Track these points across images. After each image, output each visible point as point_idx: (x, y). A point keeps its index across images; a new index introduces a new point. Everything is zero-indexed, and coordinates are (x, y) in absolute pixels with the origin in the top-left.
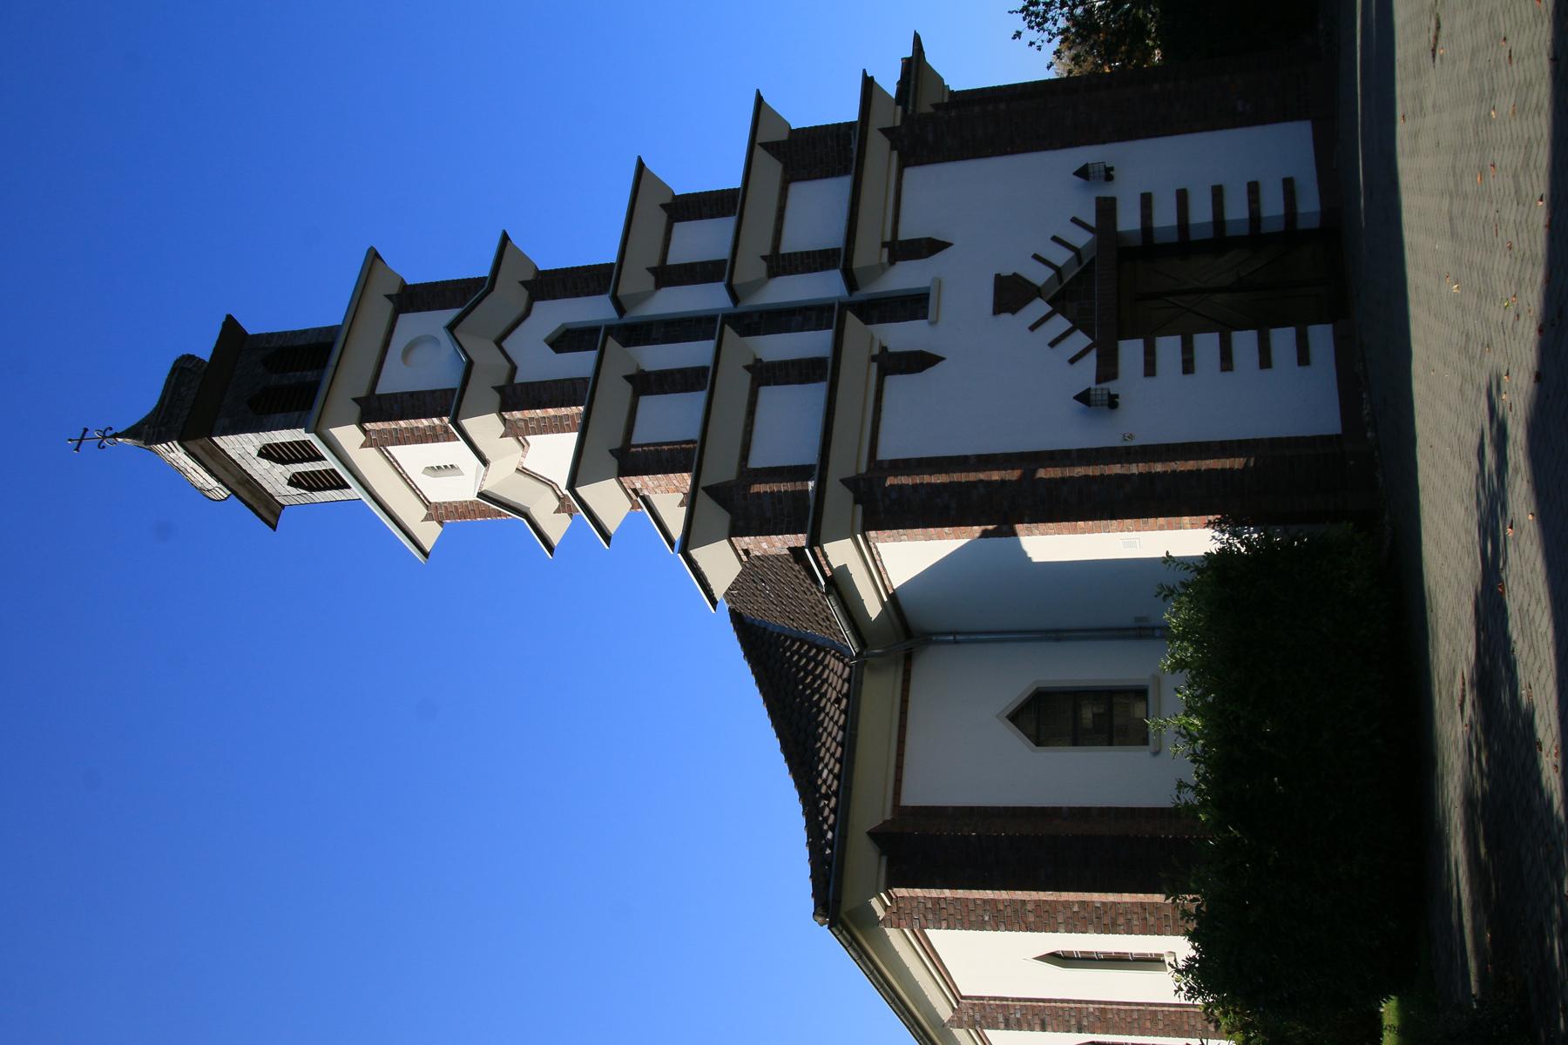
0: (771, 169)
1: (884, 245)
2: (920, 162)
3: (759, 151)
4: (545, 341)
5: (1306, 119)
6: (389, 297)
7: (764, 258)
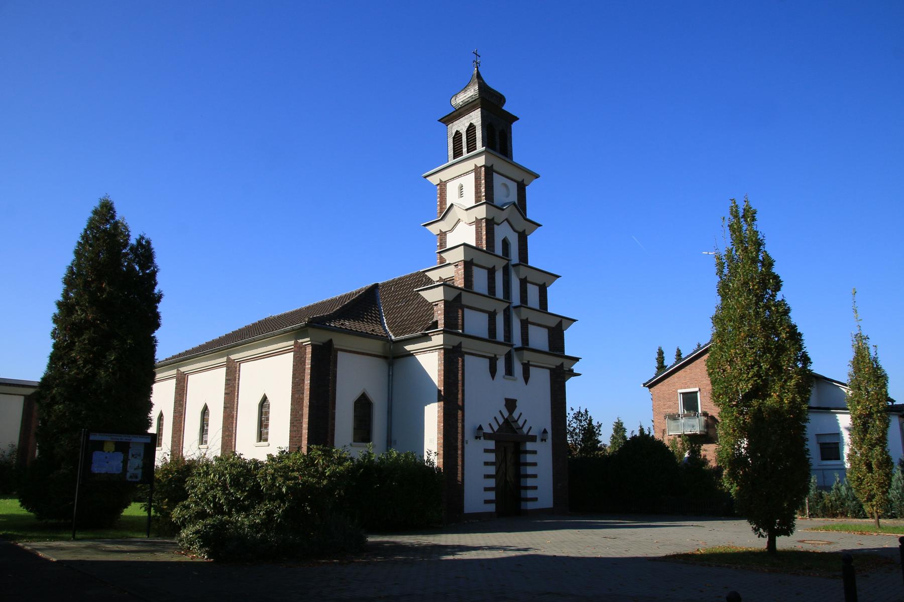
0: (553, 323)
1: (529, 361)
2: (551, 375)
5: (554, 506)
6: (523, 180)
7: (527, 319)
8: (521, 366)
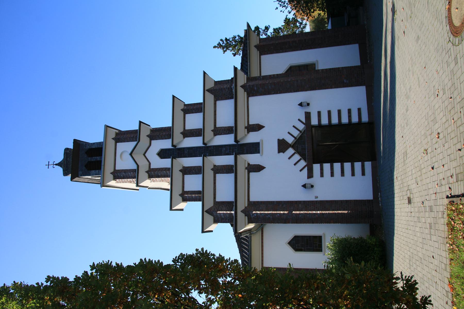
0: (210, 97)
1: (246, 128)
3: (206, 92)
4: (156, 154)
6: (113, 139)
8: (250, 133)
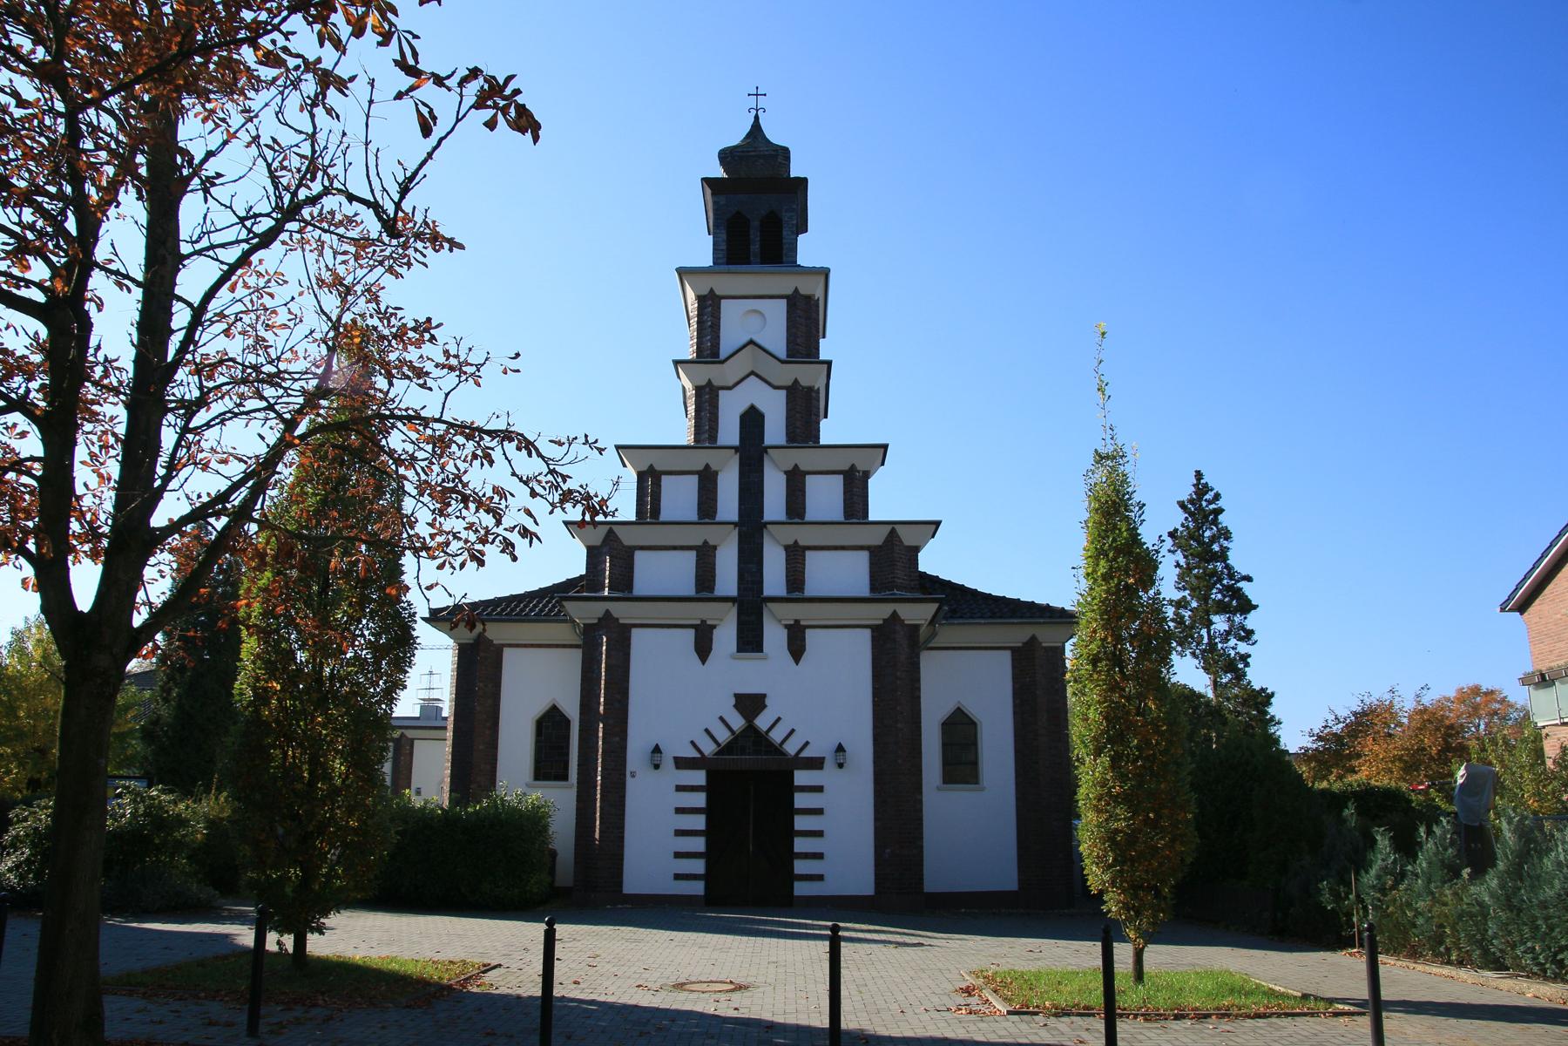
0: (877, 538)
1: (797, 621)
8: (785, 631)
